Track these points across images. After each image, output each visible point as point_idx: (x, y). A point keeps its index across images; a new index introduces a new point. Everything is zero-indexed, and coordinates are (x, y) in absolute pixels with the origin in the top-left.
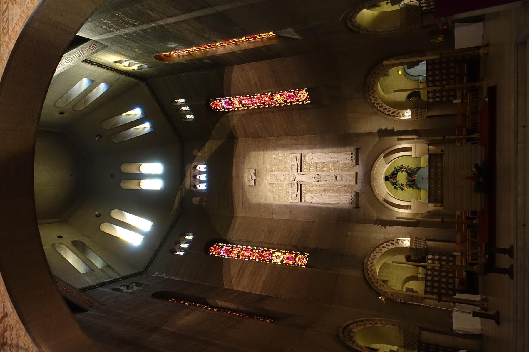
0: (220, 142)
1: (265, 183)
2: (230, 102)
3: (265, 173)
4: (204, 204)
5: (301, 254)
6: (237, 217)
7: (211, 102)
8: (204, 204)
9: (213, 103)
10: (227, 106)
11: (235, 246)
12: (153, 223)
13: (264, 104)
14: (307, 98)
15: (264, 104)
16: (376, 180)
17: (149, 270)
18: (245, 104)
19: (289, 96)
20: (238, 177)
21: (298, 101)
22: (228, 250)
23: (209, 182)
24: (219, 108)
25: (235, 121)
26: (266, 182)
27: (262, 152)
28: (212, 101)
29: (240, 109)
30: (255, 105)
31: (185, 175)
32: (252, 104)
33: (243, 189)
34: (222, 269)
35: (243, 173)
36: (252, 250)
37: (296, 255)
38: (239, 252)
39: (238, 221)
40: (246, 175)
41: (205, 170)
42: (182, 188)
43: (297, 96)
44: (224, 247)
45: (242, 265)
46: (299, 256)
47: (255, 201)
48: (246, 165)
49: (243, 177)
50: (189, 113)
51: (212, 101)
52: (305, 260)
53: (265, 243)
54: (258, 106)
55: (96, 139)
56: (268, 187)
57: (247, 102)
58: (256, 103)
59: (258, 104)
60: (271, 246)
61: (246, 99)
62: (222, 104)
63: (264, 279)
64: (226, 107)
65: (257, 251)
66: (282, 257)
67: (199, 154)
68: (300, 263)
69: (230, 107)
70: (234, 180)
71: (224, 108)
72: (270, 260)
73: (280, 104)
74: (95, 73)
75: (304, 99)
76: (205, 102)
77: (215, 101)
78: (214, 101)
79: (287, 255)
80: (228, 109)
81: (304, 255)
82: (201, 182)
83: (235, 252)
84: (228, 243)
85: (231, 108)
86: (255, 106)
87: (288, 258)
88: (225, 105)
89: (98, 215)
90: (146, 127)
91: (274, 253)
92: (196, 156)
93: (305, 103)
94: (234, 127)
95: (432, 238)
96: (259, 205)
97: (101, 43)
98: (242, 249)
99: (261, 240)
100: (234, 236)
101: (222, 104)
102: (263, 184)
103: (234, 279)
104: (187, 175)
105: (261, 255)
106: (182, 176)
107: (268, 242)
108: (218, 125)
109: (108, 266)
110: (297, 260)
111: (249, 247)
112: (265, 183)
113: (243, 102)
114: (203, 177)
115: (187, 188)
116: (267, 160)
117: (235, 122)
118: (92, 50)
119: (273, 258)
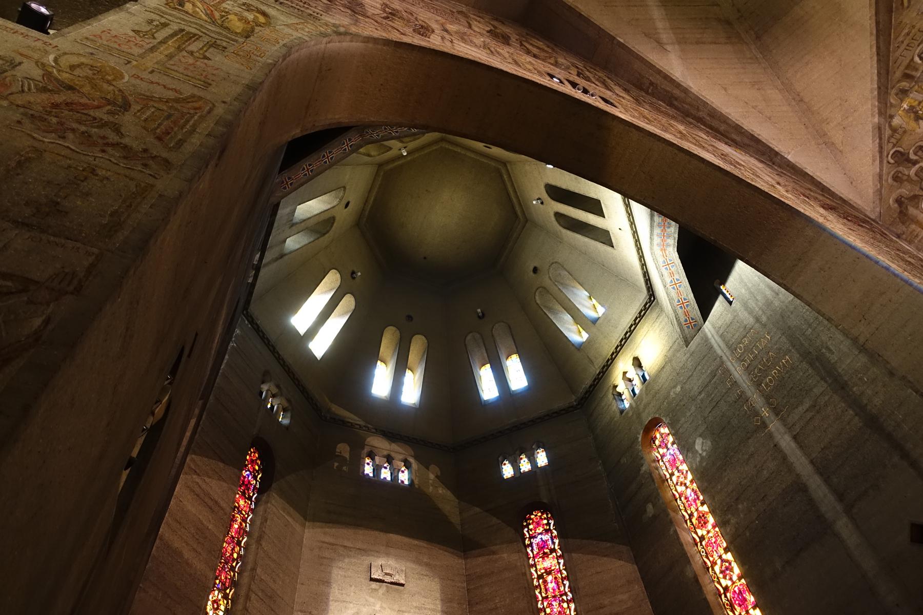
0: (455, 519)
1: (374, 605)
3: (396, 607)
4: (336, 464)
6: (304, 526)
7: (542, 514)
8: (336, 464)
9: (540, 516)
10: (538, 544)
11: (253, 507)
12: (319, 359)
17: (246, 322)
18: (545, 582)
20: (388, 545)
22: (248, 489)
23: (375, 483)
24: (531, 527)
25: (507, 556)
26: (378, 607)
27: (439, 607)
28: (545, 516)
29: (533, 570)
30: (545, 604)
31: (394, 442)
32: (547, 598)
33: (364, 551)
34: (223, 461)
35: (398, 557)
36: (239, 543)
39: (298, 528)
40: (392, 562)
42: (368, 430)
45: (222, 509)
47: (337, 574)
48: (414, 566)
49: (388, 555)
51: (545, 516)
53: (253, 578)
55: (479, 310)
57: (551, 586)
58: (550, 605)
60: (243, 592)
61: (557, 583)
62: (541, 534)
63: (187, 554)
65: (235, 556)
67: (432, 476)
69: (536, 551)
70: (383, 536)
71: (531, 537)
74: (610, 328)
76: (545, 501)
77: (545, 522)
78: (548, 519)
80: (531, 545)
83: (242, 502)
84: (260, 491)
85: (532, 551)
86: (543, 603)
88: (538, 540)
89: (355, 275)
90: (488, 389)
91: (225, 597)
92: (428, 469)
94: (494, 553)
96: (327, 583)
97: (695, 336)
99: (259, 570)
100: (274, 509)
101: (541, 534)
102: (372, 600)
104: (393, 444)
105: (227, 564)
106: (391, 436)
107: (253, 587)
108: (495, 520)
109: (282, 256)
112: (374, 603)
113: (550, 578)
115: (368, 440)
117: (505, 555)
118: (686, 321)
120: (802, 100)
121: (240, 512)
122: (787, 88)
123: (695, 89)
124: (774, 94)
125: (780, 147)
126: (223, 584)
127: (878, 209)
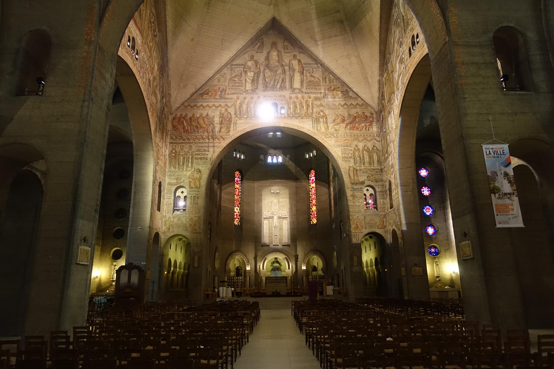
0: (294, 171)
1: (272, 199)
2: (313, 182)
5: (239, 221)
6: (254, 183)
8: (260, 162)
11: (240, 185)
13: (312, 200)
14: (313, 223)
15: (312, 200)
16: (275, 254)
18: (312, 190)
19: (314, 214)
20: (275, 183)
21: (312, 218)
22: (238, 182)
24: (311, 174)
25: (304, 183)
26: (273, 199)
27: (288, 196)
29: (310, 187)
31: (276, 150)
32: (312, 194)
33: (269, 186)
34: (229, 182)
35: (278, 186)
36: (239, 195)
37: (238, 219)
38: (237, 188)
39: (252, 184)
40: (277, 188)
41: (279, 162)
42: (268, 148)
43: (314, 218)
44: (239, 179)
46: (238, 220)
47: (263, 193)
48: (282, 187)
49: (275, 186)
50: (309, 156)
52: (237, 223)
53: (243, 202)
54: (311, 197)
56: (270, 200)
58: (312, 196)
59: (312, 197)
60: (242, 204)
63: (228, 206)
64: (311, 179)
65: (239, 198)
66: (237, 212)
67: (288, 159)
68: (235, 221)
69: (311, 181)
70: (274, 181)
71: (311, 177)
72: (235, 206)
73: (311, 209)
75: (313, 221)
79: (238, 214)
80: (310, 180)
81: (239, 222)
82: (272, 160)
83: (237, 186)
84: (241, 181)
87: (237, 215)
91: (239, 207)
92: (286, 156)
93: (311, 221)
94: (301, 182)
95: (250, 279)
96: (261, 195)
98: (239, 189)
99: (244, 200)
100: (245, 184)
102: (272, 198)
103: (226, 191)
104: (276, 151)
106: (275, 148)
107: (244, 204)
108: (302, 173)
110: (237, 219)
111: (240, 193)
114: (275, 161)
115: (269, 151)
116: (284, 200)
117: (304, 183)
119: (236, 207)
120: (362, 63)
121: (237, 188)
122: (358, 56)
123: (327, 63)
124: (354, 60)
125: (352, 86)
126: (238, 205)
127: (378, 108)
